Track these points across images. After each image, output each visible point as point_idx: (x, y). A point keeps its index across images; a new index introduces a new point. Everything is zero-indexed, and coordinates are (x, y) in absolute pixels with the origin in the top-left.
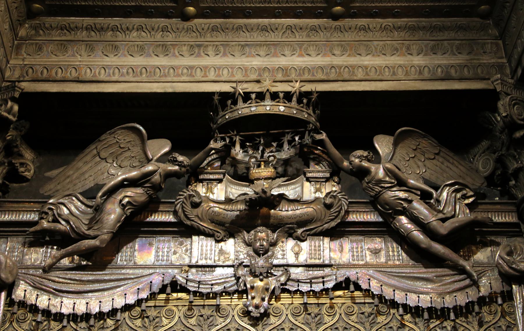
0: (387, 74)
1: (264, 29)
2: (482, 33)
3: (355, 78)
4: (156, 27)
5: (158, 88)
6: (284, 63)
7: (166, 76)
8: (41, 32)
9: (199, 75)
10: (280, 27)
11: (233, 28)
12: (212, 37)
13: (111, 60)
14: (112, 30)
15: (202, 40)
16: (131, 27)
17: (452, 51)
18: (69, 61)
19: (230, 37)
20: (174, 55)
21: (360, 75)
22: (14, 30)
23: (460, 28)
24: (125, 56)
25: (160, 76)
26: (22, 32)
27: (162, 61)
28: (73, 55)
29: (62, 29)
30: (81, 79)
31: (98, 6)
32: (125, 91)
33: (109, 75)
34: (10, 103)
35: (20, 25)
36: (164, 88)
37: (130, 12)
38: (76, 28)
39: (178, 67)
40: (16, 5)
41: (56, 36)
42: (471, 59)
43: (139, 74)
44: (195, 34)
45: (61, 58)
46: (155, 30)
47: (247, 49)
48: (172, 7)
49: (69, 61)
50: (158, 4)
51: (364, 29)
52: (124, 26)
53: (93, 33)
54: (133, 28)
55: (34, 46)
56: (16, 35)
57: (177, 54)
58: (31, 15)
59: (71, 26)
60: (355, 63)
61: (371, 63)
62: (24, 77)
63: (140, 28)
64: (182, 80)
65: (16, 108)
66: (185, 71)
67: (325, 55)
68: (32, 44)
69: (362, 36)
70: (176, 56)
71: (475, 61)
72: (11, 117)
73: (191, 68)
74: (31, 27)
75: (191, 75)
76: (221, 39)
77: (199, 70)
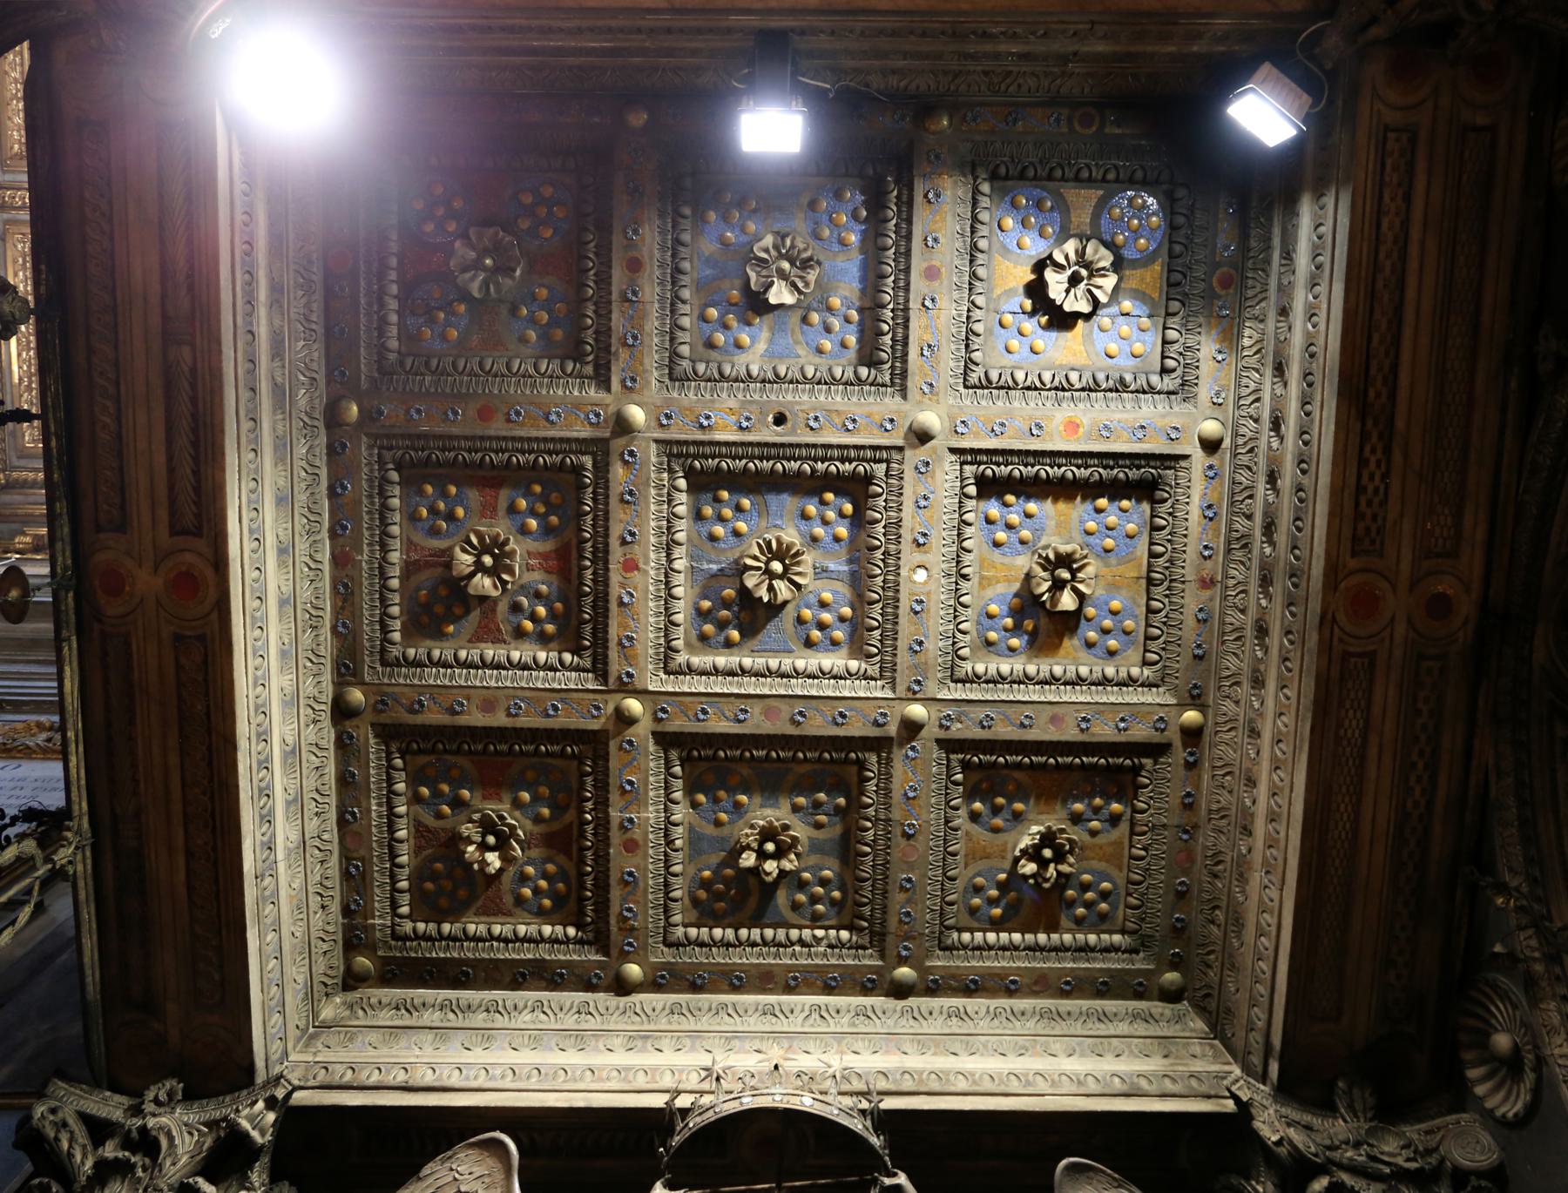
0: (1015, 1086)
1: (769, 1012)
2: (1178, 1027)
3: (952, 1089)
4: (568, 1005)
5: (557, 1100)
6: (809, 1064)
7: (575, 1081)
8: (361, 1013)
9: (641, 1081)
10: (799, 1008)
11: (710, 1009)
12: (670, 1023)
13: (478, 1056)
14: (487, 1011)
15: (652, 1027)
16: (521, 1005)
17: (1131, 1052)
18: (397, 1056)
19: (705, 1023)
20: (596, 1049)
21: (962, 1085)
22: (310, 997)
23: (1136, 1016)
24: (503, 1049)
25: (564, 1081)
26: (327, 1013)
27: (572, 1058)
28: (408, 1048)
29: (397, 1008)
30: (411, 1083)
31: (467, 962)
32: (493, 1105)
33: (467, 1078)
34: (260, 1105)
35: (327, 995)
36: (570, 1100)
37: (523, 975)
38: (424, 1005)
39: (602, 1068)
40: (325, 947)
41: (386, 1017)
42: (1172, 1065)
43: (524, 1078)
44: (638, 1018)
45: (384, 1051)
46: (565, 1010)
47: (736, 1043)
48: (600, 964)
49: (397, 1056)
50: (575, 957)
51: (962, 1015)
52: (509, 1004)
53: (451, 1016)
54: (526, 1007)
55: (342, 1036)
56: (315, 1015)
57: (603, 1048)
58: (351, 980)
59: (416, 1001)
60: (949, 1066)
61: (980, 1066)
62: (308, 1080)
63: (539, 1006)
64: (606, 1088)
65: (271, 1117)
66: (615, 1073)
67: (887, 1052)
68: (339, 1032)
69: (955, 1025)
70: (600, 1051)
71: (1180, 1068)
72: (255, 1134)
73: (628, 1069)
74: (344, 1003)
75: (625, 1080)
76: (688, 1028)
77: (642, 1072)
